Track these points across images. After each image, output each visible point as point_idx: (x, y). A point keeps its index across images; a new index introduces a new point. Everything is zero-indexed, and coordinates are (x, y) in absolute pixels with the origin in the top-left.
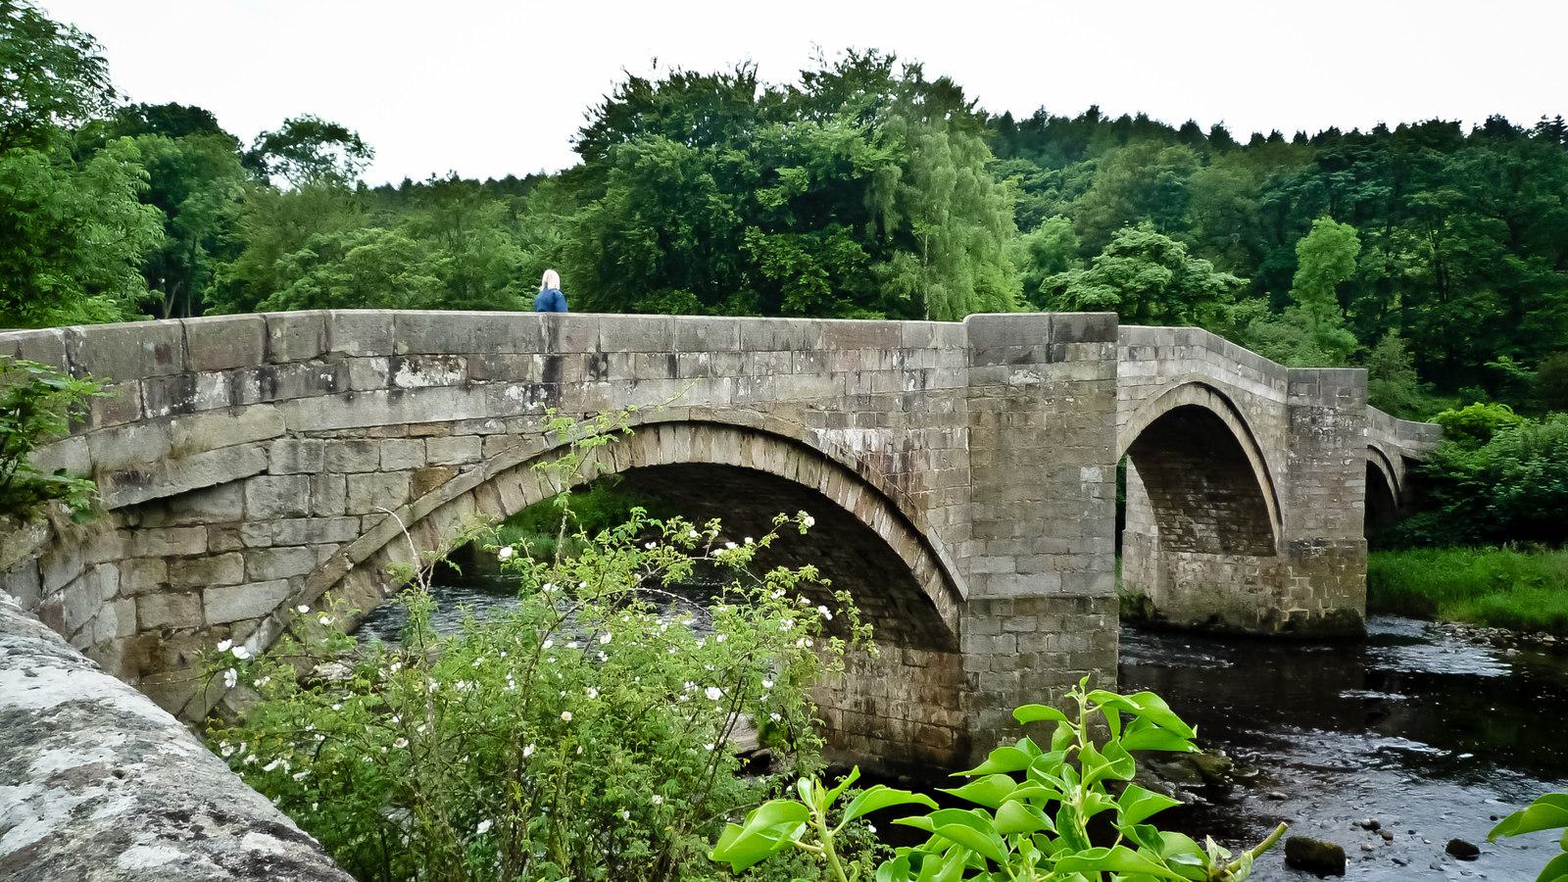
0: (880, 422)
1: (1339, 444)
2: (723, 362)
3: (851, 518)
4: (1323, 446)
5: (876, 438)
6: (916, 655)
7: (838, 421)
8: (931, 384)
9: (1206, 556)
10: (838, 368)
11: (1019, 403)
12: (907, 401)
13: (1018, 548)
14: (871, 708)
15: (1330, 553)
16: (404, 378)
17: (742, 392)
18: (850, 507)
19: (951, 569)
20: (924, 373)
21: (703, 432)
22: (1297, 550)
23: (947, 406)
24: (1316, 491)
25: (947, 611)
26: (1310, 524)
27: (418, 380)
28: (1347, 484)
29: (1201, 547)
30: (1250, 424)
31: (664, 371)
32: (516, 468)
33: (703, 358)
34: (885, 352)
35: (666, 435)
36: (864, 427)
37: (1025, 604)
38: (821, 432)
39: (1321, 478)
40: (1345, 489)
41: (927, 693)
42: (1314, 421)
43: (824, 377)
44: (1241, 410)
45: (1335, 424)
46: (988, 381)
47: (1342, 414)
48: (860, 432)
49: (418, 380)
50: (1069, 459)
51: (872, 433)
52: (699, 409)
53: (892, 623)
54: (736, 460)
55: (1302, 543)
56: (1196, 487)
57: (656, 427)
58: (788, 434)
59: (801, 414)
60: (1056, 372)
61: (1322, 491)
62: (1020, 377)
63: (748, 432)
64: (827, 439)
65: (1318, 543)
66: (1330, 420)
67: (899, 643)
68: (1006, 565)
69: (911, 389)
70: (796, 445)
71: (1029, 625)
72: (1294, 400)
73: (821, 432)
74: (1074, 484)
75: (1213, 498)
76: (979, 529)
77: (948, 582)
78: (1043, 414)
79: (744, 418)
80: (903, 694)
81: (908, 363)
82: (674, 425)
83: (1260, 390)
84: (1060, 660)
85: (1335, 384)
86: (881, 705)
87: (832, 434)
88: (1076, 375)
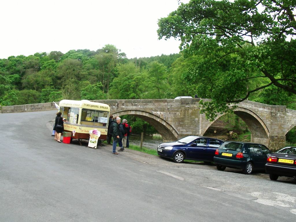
0: (163, 111)
1: (281, 119)
4: (278, 119)
5: (162, 113)
7: (156, 111)
8: (173, 107)
9: (259, 138)
10: (156, 105)
11: (186, 110)
12: (168, 109)
13: (186, 128)
15: (278, 138)
19: (176, 130)
20: (172, 105)
21: (137, 111)
22: (272, 138)
23: (176, 109)
24: (276, 127)
25: (176, 136)
26: (275, 133)
28: (282, 126)
29: (258, 137)
30: (258, 115)
31: (131, 105)
32: (114, 114)
33: (136, 104)
35: (132, 112)
36: (161, 111)
38: (153, 112)
39: (277, 125)
40: (282, 127)
42: (276, 115)
43: (154, 105)
44: (254, 112)
45: (280, 115)
46: (183, 107)
47: (281, 114)
48: (160, 112)
50: (194, 117)
54: (141, 114)
55: (273, 136)
57: (131, 110)
58: (148, 112)
60: (192, 106)
61: (277, 127)
62: (187, 106)
64: (154, 113)
65: (276, 137)
66: (279, 115)
68: (185, 130)
69: (169, 107)
70: (150, 113)
72: (272, 111)
73: (153, 112)
75: (257, 128)
76: (181, 125)
77: (176, 132)
78: (190, 111)
82: (133, 110)
83: (261, 109)
85: (280, 108)
87: (155, 112)
88: (195, 106)
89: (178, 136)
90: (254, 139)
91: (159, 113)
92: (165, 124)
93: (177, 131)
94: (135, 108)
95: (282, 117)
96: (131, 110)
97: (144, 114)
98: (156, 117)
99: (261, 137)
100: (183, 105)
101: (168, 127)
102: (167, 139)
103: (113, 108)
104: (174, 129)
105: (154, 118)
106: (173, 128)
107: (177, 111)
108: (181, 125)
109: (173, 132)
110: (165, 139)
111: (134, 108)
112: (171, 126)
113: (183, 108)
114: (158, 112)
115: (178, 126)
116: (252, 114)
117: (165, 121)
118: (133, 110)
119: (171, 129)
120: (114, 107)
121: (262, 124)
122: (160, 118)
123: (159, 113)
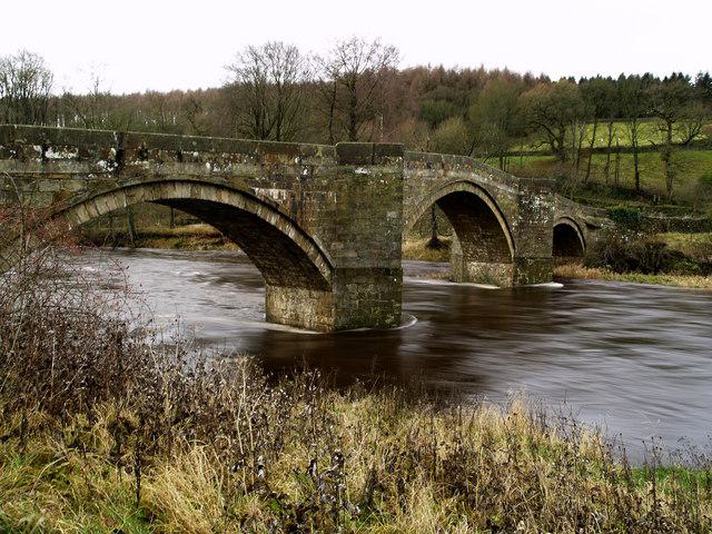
2: (206, 156)
3: (274, 228)
6: (315, 294)
7: (266, 185)
9: (483, 264)
12: (303, 178)
14: (297, 317)
16: (49, 154)
17: (215, 170)
18: (273, 222)
19: (327, 255)
23: (325, 182)
25: (326, 273)
27: (56, 156)
29: (481, 259)
33: (196, 154)
34: (291, 156)
37: (361, 272)
41: (319, 310)
46: (345, 172)
49: (56, 156)
51: (284, 192)
52: (193, 176)
53: (304, 279)
54: (214, 198)
56: (477, 232)
59: (246, 181)
62: (360, 171)
63: (220, 187)
65: (531, 258)
66: (538, 202)
67: (308, 288)
69: (305, 173)
71: (364, 280)
74: (383, 218)
75: (484, 237)
79: (217, 180)
80: (310, 311)
81: (304, 162)
83: (502, 187)
84: (377, 295)
86: (301, 316)
89: (331, 275)
90: (469, 265)
91: (274, 193)
92: (292, 234)
93: (329, 257)
94: (191, 172)
95: (544, 208)
96: (173, 182)
97: (225, 198)
98: (266, 210)
99: (492, 261)
100: (347, 167)
101: (300, 242)
102: (282, 284)
103: (98, 172)
104: (320, 251)
105: (260, 211)
106: (317, 247)
107: (327, 188)
108: (340, 239)
109: (318, 262)
110: (275, 285)
111: (190, 170)
112: (312, 241)
113: (348, 178)
114: (272, 191)
115: (332, 240)
116: (486, 199)
117: (294, 224)
118: (182, 182)
119: (311, 251)
120: (102, 163)
121: (503, 226)
122: (279, 213)
123: (274, 193)
